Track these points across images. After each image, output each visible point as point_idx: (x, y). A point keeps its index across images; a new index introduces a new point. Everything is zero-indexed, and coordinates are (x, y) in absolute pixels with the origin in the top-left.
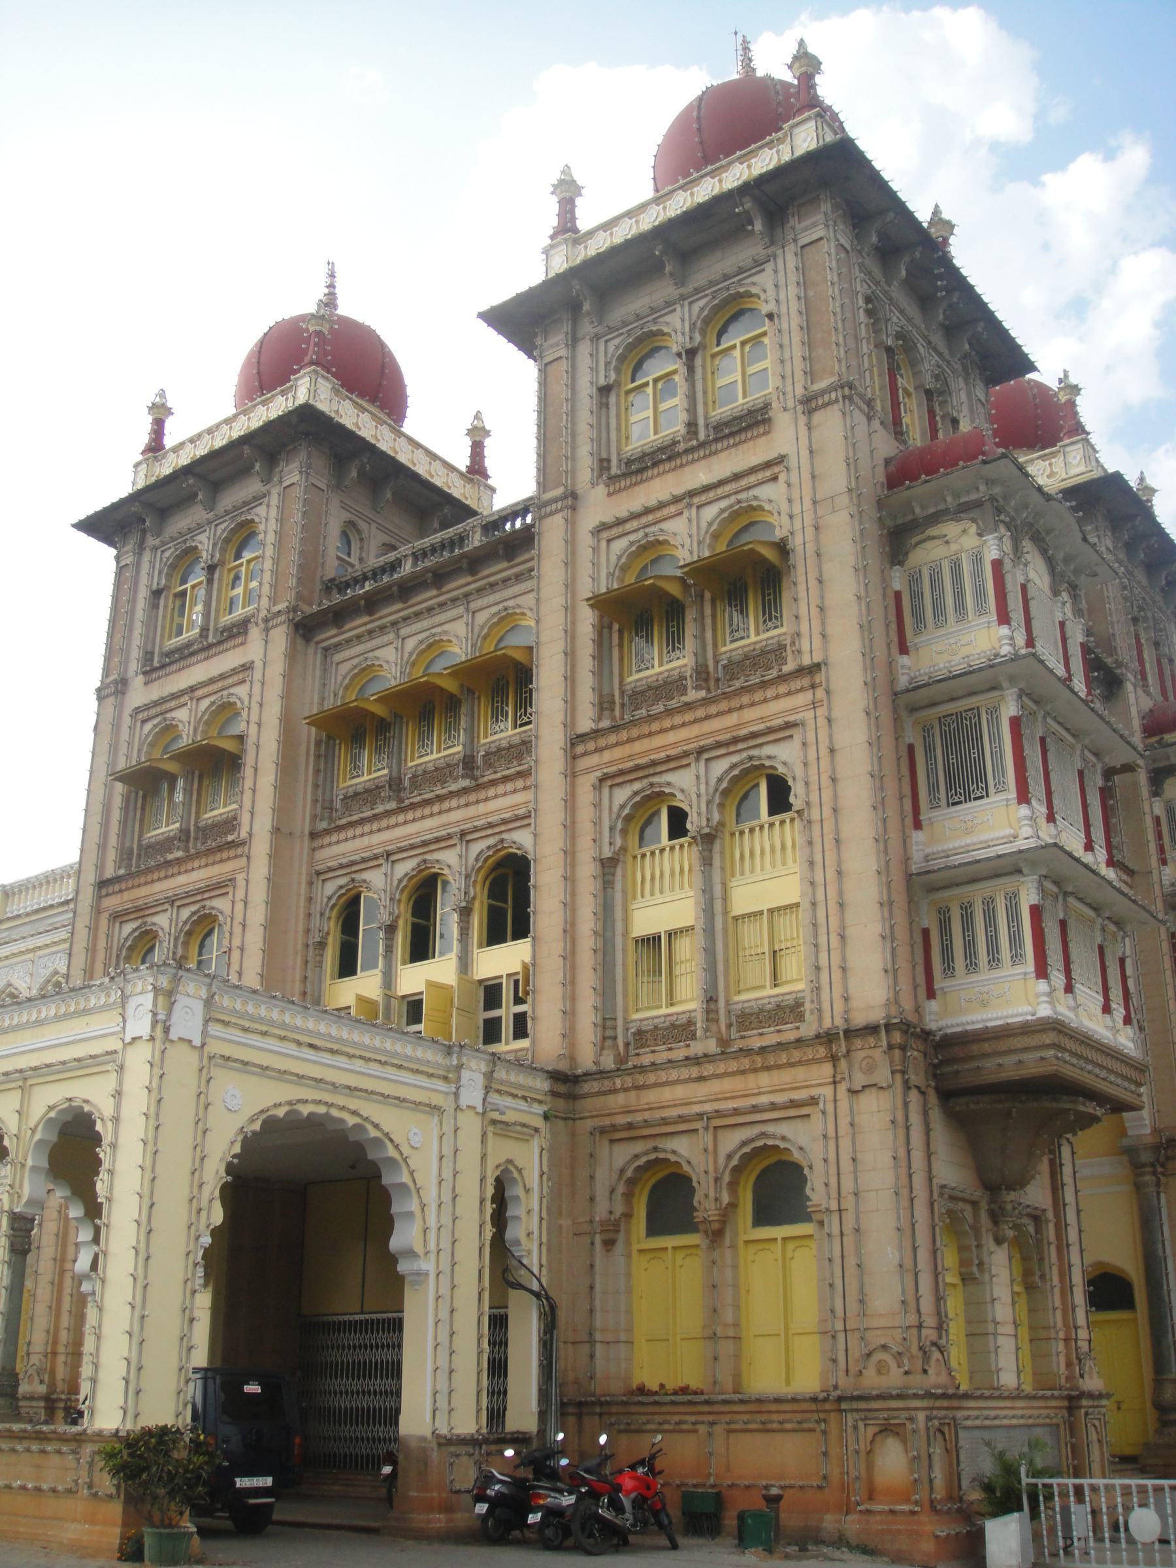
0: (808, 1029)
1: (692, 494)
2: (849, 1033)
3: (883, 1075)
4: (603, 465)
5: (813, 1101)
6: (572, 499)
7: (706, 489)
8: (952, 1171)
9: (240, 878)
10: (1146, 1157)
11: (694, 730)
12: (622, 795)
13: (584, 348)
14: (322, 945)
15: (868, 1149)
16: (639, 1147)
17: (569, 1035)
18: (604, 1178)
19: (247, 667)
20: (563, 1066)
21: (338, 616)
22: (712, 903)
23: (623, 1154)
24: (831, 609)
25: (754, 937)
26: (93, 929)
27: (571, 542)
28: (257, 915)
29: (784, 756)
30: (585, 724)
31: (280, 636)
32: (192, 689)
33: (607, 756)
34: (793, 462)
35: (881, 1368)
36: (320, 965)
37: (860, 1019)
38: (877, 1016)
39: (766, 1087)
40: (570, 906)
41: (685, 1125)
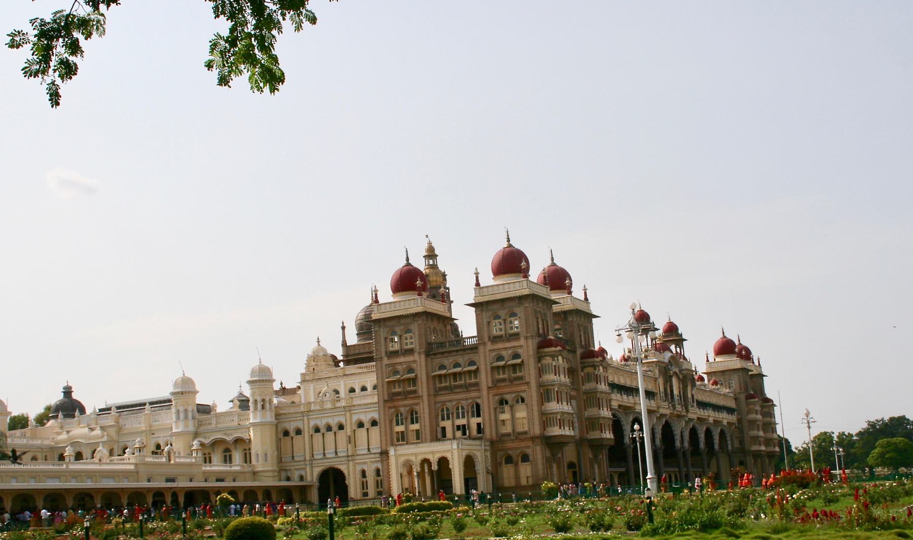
0: (529, 436)
4: (489, 337)
6: (484, 344)
8: (548, 455)
12: (497, 398)
13: (484, 313)
15: (538, 453)
17: (491, 435)
18: (498, 457)
19: (415, 361)
21: (435, 354)
24: (530, 372)
25: (519, 421)
26: (384, 410)
27: (485, 353)
28: (427, 411)
29: (524, 395)
30: (490, 385)
31: (423, 357)
39: (523, 444)
40: (490, 415)
41: (512, 449)
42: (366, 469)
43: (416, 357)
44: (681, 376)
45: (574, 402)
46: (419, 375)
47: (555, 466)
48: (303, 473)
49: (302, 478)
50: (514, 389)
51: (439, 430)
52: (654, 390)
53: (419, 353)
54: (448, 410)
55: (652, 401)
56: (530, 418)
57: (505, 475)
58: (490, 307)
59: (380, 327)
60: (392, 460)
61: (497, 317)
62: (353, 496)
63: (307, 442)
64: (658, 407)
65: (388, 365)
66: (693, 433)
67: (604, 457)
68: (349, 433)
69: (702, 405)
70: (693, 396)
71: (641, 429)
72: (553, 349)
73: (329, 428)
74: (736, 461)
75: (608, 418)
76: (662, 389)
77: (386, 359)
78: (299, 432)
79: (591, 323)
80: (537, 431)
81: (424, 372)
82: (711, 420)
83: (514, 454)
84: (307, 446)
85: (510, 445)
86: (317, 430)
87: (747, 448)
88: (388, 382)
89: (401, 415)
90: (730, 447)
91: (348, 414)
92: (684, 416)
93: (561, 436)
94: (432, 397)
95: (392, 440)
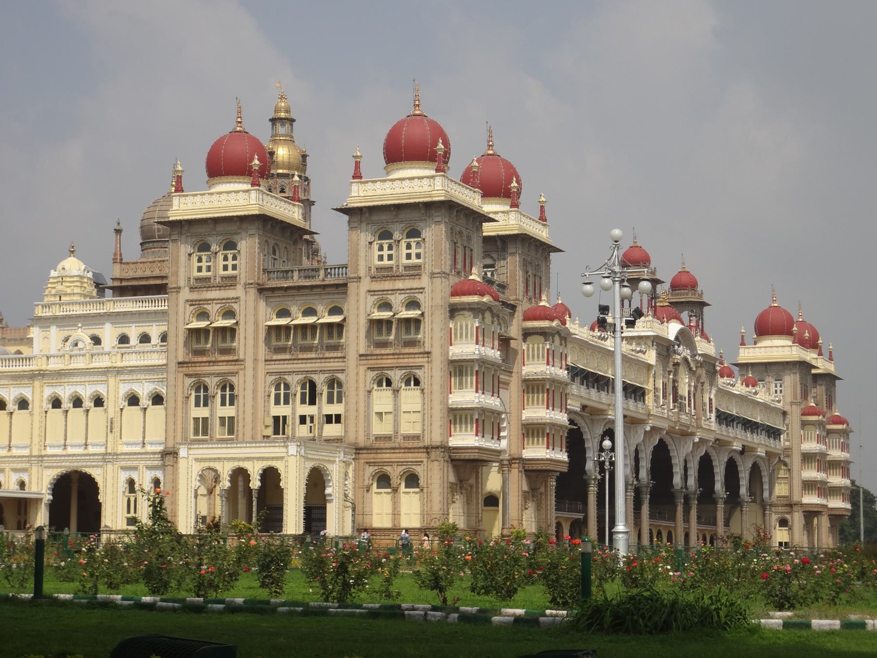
0: (421, 445)
1: (398, 290)
2: (432, 448)
5: (422, 462)
8: (452, 479)
9: (241, 372)
11: (395, 361)
14: (269, 396)
15: (436, 475)
16: (376, 468)
19: (237, 298)
23: (371, 470)
28: (250, 386)
29: (419, 373)
31: (252, 292)
33: (370, 362)
35: (435, 522)
36: (269, 401)
37: (434, 444)
38: (438, 444)
39: (411, 457)
41: (390, 464)
42: (136, 480)
43: (238, 291)
46: (242, 323)
48: (25, 477)
49: (22, 485)
50: (404, 361)
51: (270, 422)
53: (247, 285)
54: (287, 387)
56: (425, 414)
57: (376, 510)
58: (375, 218)
59: (181, 234)
60: (182, 464)
61: (386, 235)
62: (109, 524)
63: (36, 425)
65: (191, 302)
66: (706, 466)
68: (111, 414)
69: (724, 418)
71: (613, 449)
72: (475, 299)
73: (77, 402)
74: (774, 518)
75: (561, 426)
77: (187, 288)
78: (23, 404)
79: (547, 259)
80: (435, 437)
81: (251, 319)
82: (737, 446)
83: (395, 472)
84: (36, 432)
85: (386, 456)
86: (56, 403)
87: (796, 498)
88: (189, 329)
89: (206, 389)
91: (112, 380)
93: (479, 449)
94: (261, 365)
95: (185, 430)
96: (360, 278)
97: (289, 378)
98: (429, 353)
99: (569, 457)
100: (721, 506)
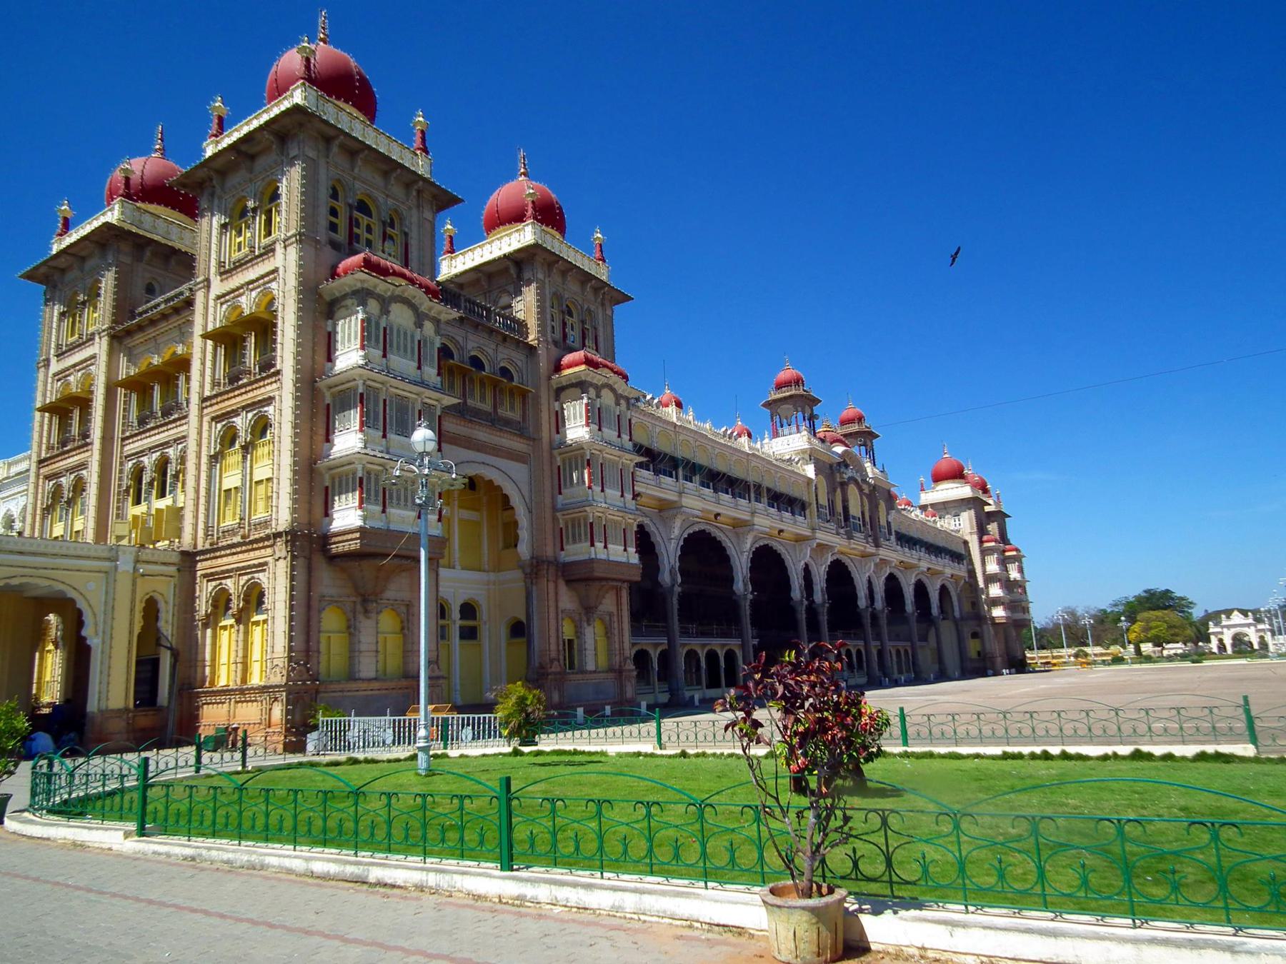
3: (284, 554)
5: (266, 564)
7: (252, 282)
10: (528, 570)
20: (190, 549)
21: (129, 333)
22: (247, 475)
30: (207, 393)
31: (105, 341)
32: (75, 366)
34: (281, 271)
38: (281, 529)
41: (226, 574)
44: (866, 491)
45: (519, 471)
47: (366, 625)
52: (805, 498)
55: (800, 519)
64: (813, 529)
67: (615, 605)
70: (889, 523)
74: (967, 630)
76: (823, 500)
77: (53, 360)
90: (957, 614)
92: (873, 555)
96: (208, 280)
97: (145, 459)
98: (278, 373)
99: (641, 559)
100: (914, 626)
